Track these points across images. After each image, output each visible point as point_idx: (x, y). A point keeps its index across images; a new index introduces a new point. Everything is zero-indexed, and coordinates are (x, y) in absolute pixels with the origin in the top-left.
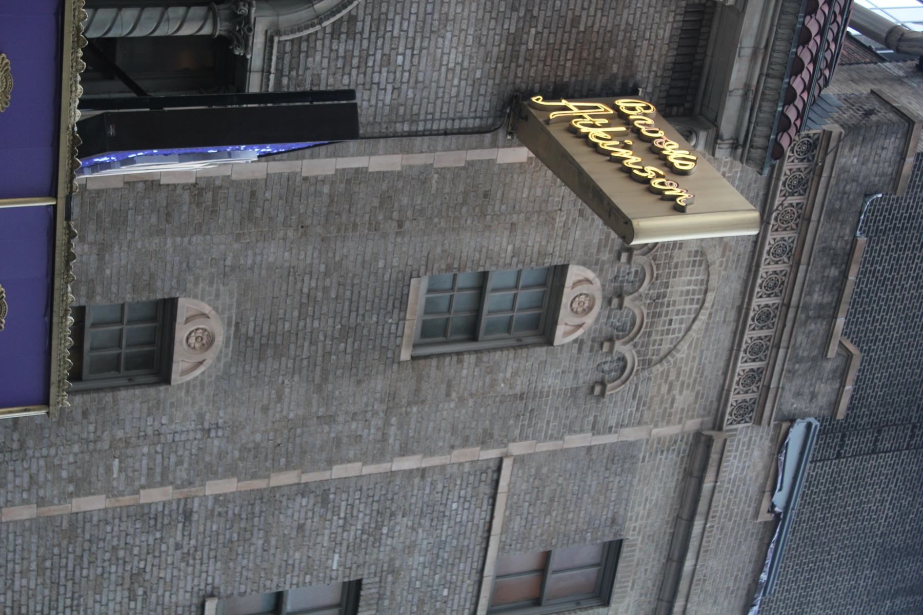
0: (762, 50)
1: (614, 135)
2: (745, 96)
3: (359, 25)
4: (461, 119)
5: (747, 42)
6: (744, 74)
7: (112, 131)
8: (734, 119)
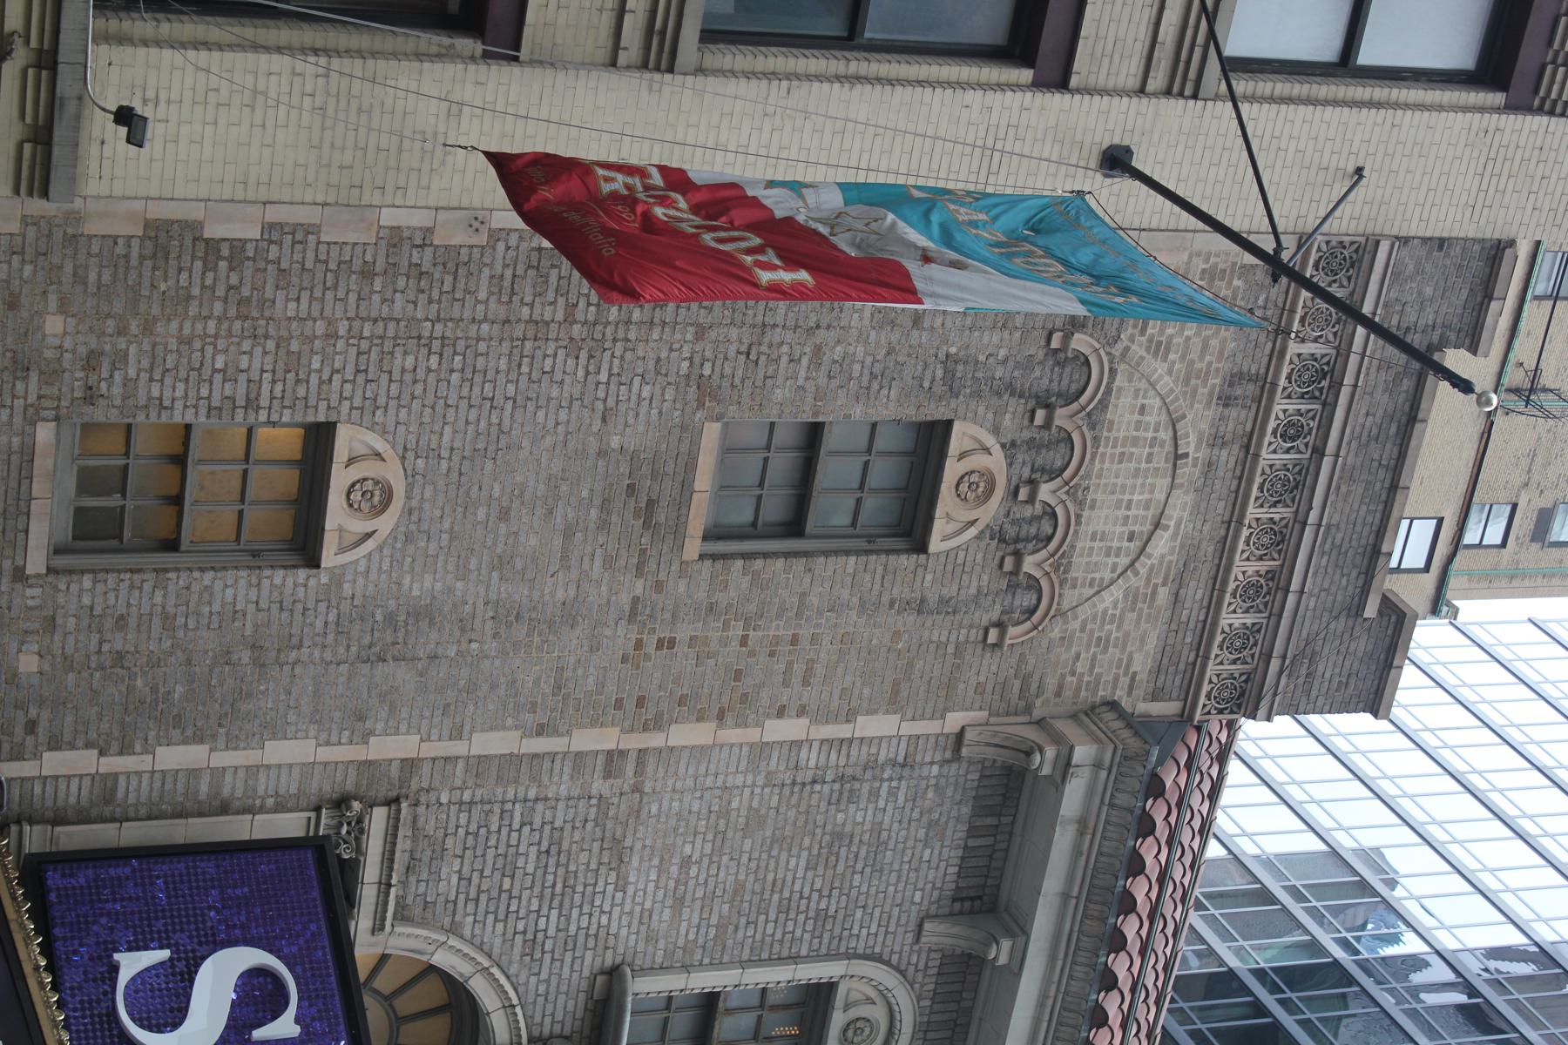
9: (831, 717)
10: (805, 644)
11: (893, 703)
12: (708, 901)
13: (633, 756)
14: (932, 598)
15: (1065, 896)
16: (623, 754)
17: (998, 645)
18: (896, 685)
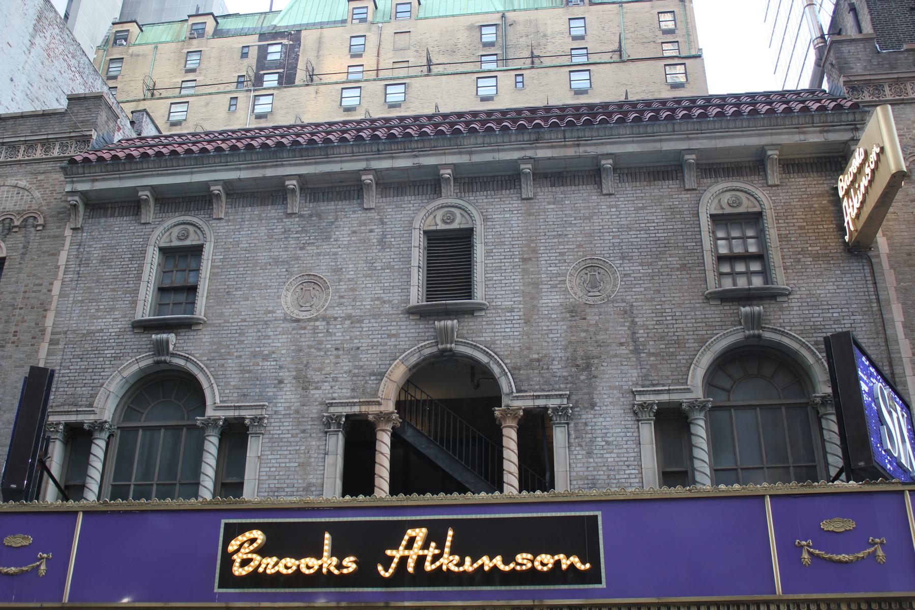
0: (799, 129)
1: (855, 193)
2: (827, 131)
3: (819, 339)
4: (865, 277)
5: (797, 138)
6: (814, 135)
7: (862, 464)
8: (841, 133)
9: (56, 274)
10: (27, 289)
11: (56, 254)
12: (114, 299)
13: (53, 337)
14: (22, 251)
15: (120, 178)
16: (51, 340)
17: (44, 226)
18: (49, 255)
